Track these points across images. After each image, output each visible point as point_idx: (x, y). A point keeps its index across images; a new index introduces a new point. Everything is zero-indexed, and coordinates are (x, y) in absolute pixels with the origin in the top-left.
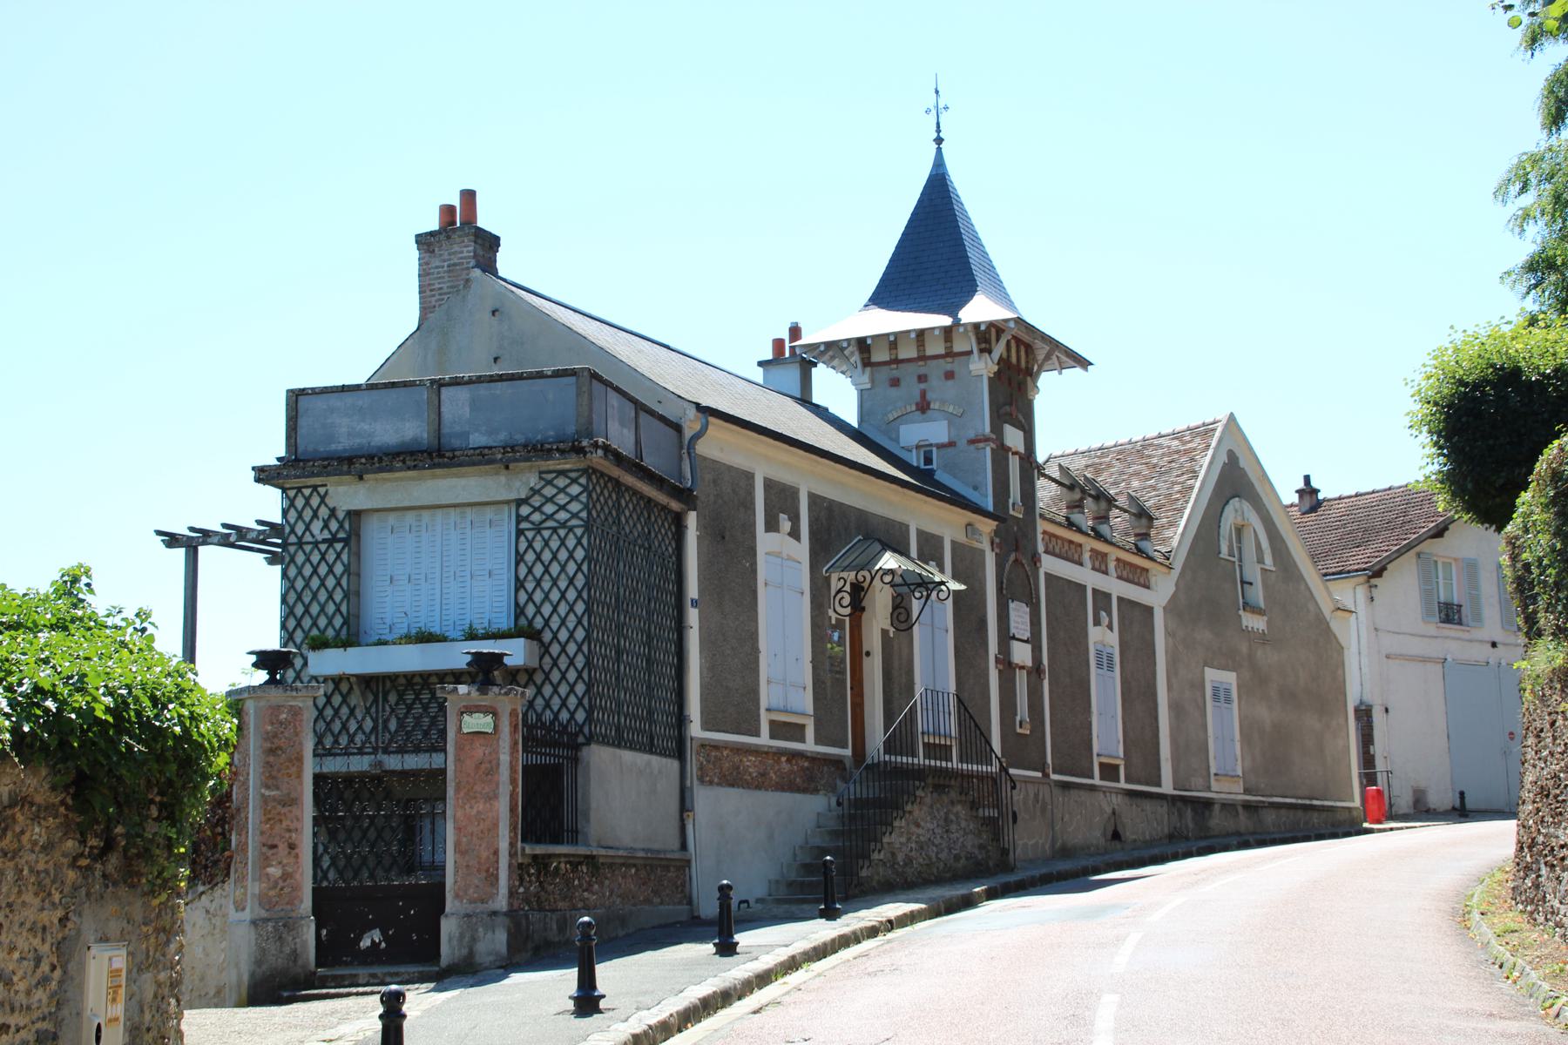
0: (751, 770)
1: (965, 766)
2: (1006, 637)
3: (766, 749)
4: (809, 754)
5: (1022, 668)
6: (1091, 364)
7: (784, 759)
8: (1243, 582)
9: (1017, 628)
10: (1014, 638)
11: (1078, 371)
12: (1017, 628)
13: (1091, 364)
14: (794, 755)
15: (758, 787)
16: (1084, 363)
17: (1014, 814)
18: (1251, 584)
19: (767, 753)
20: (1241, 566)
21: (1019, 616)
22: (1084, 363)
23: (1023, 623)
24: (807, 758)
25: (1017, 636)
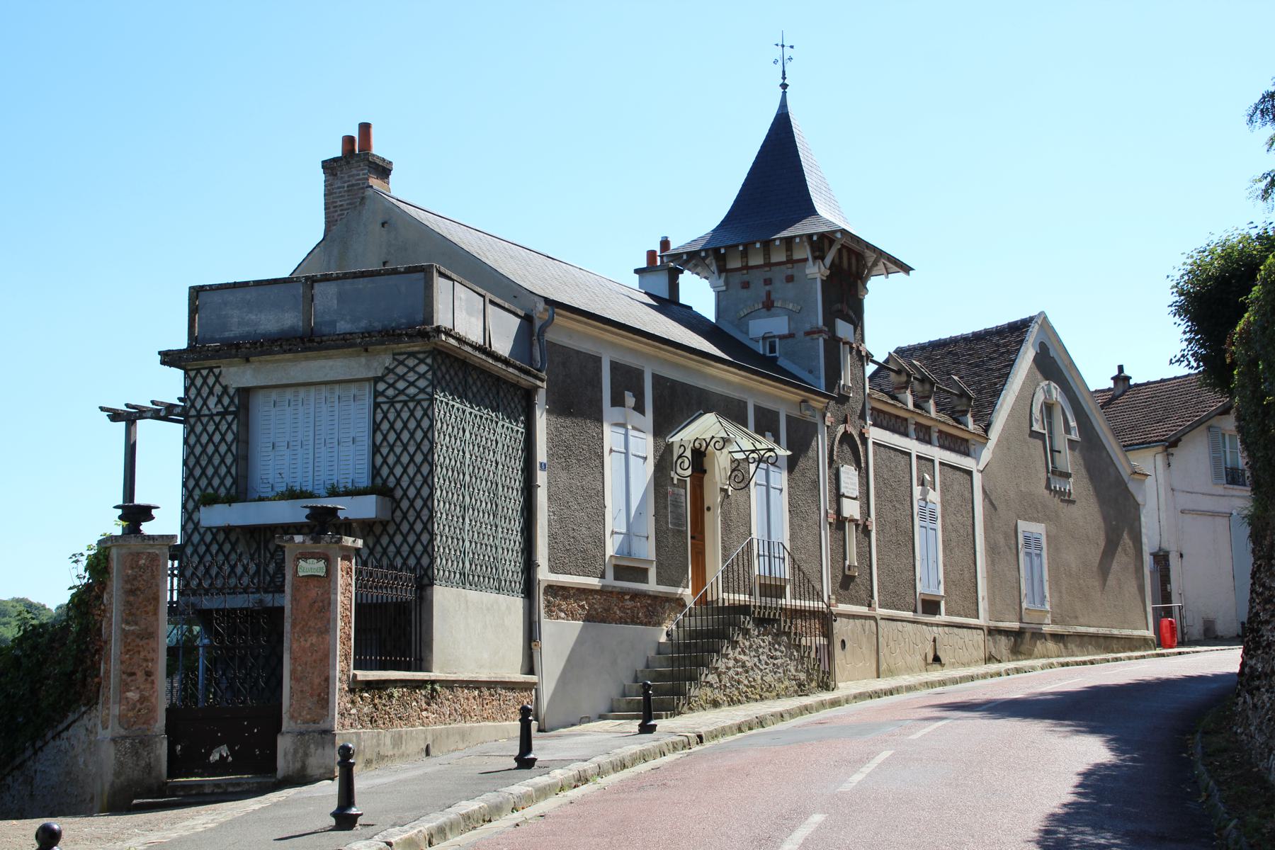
0: (596, 606)
1: (798, 602)
2: (838, 496)
3: (610, 589)
4: (651, 593)
5: (852, 520)
6: (912, 269)
7: (627, 597)
8: (1052, 451)
9: (847, 487)
10: (843, 495)
11: (902, 275)
12: (847, 487)
13: (912, 269)
14: (636, 595)
15: (603, 621)
16: (906, 269)
17: (843, 642)
18: (1059, 452)
19: (611, 592)
20: (1051, 438)
21: (849, 478)
22: (906, 269)
23: (852, 484)
24: (650, 596)
25: (846, 494)
